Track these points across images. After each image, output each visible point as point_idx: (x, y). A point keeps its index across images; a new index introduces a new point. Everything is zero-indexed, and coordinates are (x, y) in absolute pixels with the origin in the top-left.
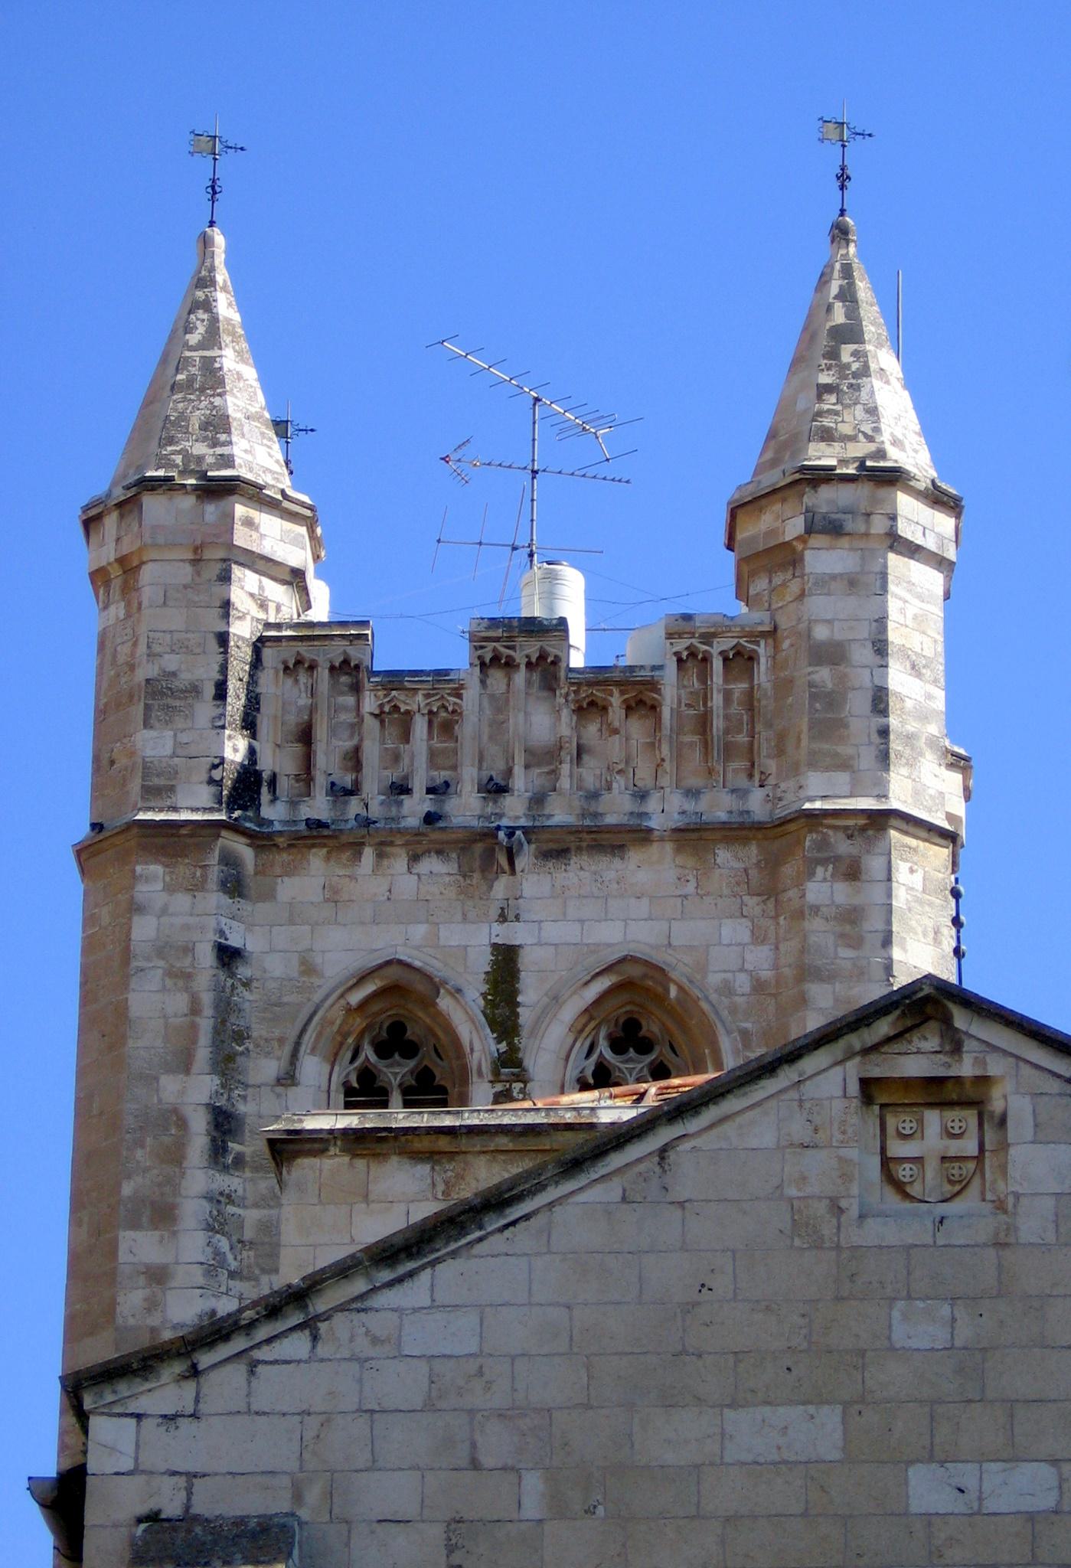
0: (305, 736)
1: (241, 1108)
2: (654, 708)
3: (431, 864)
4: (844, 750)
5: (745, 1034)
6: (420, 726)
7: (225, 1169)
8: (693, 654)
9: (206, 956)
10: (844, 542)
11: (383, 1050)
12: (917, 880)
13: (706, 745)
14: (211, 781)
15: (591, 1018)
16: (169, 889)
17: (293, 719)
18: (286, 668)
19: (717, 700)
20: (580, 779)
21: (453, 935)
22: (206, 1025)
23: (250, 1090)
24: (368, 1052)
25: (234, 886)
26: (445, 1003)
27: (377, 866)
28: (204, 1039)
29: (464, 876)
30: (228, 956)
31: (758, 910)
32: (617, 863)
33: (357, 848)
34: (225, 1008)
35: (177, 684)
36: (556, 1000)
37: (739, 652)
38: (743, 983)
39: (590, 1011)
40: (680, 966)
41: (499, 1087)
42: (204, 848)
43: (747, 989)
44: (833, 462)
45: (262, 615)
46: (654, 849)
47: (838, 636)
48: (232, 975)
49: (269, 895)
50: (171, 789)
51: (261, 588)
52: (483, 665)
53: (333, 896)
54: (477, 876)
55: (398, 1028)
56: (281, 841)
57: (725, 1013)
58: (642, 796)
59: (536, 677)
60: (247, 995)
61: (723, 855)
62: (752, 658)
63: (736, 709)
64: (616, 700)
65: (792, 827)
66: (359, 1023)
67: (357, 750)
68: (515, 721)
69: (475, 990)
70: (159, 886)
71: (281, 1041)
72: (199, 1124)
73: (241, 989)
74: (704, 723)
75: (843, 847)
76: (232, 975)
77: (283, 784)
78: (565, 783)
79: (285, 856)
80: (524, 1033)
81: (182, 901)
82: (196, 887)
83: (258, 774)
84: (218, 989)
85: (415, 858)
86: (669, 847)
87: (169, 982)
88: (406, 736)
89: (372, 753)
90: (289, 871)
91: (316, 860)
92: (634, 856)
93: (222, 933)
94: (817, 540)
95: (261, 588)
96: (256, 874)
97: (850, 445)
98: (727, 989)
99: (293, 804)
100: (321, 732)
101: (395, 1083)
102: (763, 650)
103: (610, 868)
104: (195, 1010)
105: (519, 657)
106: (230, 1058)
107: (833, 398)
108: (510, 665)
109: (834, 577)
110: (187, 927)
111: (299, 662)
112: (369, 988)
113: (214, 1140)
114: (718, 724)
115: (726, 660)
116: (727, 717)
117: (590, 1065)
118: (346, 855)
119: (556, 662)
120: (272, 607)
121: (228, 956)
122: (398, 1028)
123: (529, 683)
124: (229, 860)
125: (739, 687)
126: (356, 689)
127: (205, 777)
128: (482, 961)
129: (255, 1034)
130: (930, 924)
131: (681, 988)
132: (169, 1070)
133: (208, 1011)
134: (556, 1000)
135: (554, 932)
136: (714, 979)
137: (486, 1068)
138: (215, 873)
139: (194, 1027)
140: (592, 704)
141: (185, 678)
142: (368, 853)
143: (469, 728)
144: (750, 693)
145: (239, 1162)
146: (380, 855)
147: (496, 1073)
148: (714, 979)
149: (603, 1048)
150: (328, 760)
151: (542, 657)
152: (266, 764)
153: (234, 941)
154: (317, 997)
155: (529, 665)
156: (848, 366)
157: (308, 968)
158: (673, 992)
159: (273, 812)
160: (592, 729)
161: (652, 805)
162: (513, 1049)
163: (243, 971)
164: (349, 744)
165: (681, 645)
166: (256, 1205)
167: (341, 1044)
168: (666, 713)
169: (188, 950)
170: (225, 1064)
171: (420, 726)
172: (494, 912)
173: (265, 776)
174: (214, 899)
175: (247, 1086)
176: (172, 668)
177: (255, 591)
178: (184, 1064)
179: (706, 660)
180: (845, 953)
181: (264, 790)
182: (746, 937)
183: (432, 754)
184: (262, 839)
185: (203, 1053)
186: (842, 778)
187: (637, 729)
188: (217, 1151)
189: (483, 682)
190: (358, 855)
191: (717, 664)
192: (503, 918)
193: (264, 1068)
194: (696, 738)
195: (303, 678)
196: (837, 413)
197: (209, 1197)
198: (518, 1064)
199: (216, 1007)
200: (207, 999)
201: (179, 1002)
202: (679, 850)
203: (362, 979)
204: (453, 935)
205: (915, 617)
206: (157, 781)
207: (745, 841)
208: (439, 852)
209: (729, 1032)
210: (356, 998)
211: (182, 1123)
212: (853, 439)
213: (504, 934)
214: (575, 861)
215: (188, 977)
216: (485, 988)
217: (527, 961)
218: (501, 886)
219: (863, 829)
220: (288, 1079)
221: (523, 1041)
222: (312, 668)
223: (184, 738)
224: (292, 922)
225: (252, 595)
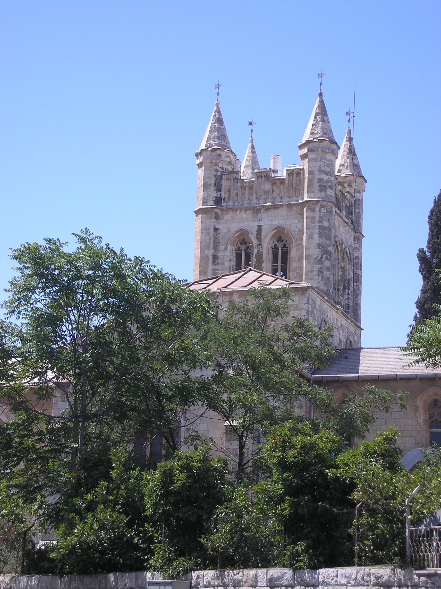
0: (229, 191)
1: (218, 254)
2: (284, 183)
3: (248, 212)
4: (313, 189)
5: (297, 238)
6: (247, 189)
7: (215, 265)
8: (291, 173)
9: (212, 230)
10: (314, 153)
11: (241, 244)
12: (325, 211)
13: (293, 189)
14: (213, 200)
15: (273, 237)
16: (206, 219)
17: (227, 188)
18: (227, 179)
19: (294, 181)
20: (273, 196)
21: (251, 224)
22: (212, 241)
23: (220, 252)
24: (239, 244)
25: (217, 217)
26: (250, 235)
27: (240, 213)
28: (212, 244)
29: (253, 214)
30: (216, 230)
31: (299, 217)
32: (277, 210)
33: (237, 210)
34: (215, 238)
35: (208, 184)
36: (267, 235)
37: (298, 172)
38: (297, 230)
39: (273, 236)
40: (287, 227)
41: (258, 249)
42: (212, 211)
43: (297, 231)
44: (312, 139)
45: (223, 171)
46: (283, 208)
47: (312, 170)
48: (217, 233)
49: (223, 218)
50: (207, 202)
51: (222, 166)
52: (257, 177)
53: (233, 218)
54: (255, 214)
55: (244, 240)
56: (225, 209)
57: (294, 235)
58: (282, 198)
59: (266, 178)
60: (220, 236)
61: (294, 208)
62: (300, 173)
63: (298, 182)
64: (278, 182)
65: (304, 203)
66: (237, 239)
67: (238, 192)
68: (262, 186)
69: (255, 233)
70: (205, 218)
71: (225, 243)
72: (211, 258)
73: (218, 235)
74: (292, 185)
75: (313, 206)
76: (217, 233)
77: (226, 199)
78: (270, 197)
79: (226, 212)
80: (262, 240)
81: (208, 221)
82: (211, 218)
83: (221, 198)
84: (214, 235)
85: (246, 211)
86: (286, 207)
87: (206, 235)
88: (245, 190)
89: (239, 193)
90: (226, 214)
91: (230, 212)
92: (280, 209)
93: (215, 226)
94: (310, 153)
95: (222, 166)
96: (221, 215)
97: (316, 135)
98: (294, 231)
99: (227, 203)
100: (232, 190)
101: (243, 249)
102: (302, 172)
103: (276, 211)
104: (210, 239)
105: (263, 176)
106: (216, 246)
107: (314, 126)
108: (262, 177)
109: (312, 159)
110: (209, 225)
111: (228, 178)
112: (238, 234)
113: (213, 260)
114: (294, 185)
115: (296, 174)
116: (296, 184)
117: (274, 244)
118: (235, 211)
119: (269, 176)
120: (224, 169)
121: (216, 230)
122: (244, 240)
123: (265, 179)
124: (216, 213)
125: (298, 179)
126: (238, 182)
127: (212, 199)
128: (256, 228)
129: (221, 242)
130: (327, 218)
131: (287, 231)
132: (207, 249)
133: (212, 239)
134: (267, 235)
135: (268, 223)
136: (292, 229)
137: (256, 246)
138: (214, 216)
139: (210, 242)
140: (275, 183)
141: (209, 183)
142: (238, 210)
143: (254, 189)
144: (300, 179)
145: (218, 263)
146: (240, 211)
147: (257, 247)
148: (292, 229)
149: (276, 242)
150: (233, 194)
151: (267, 175)
152: (223, 197)
153: (217, 227)
154: (230, 235)
155: (265, 177)
156: (318, 120)
157: (229, 231)
158: (286, 232)
159: (224, 204)
160: (275, 187)
161: (283, 200)
162: (260, 243)
163: (218, 232)
164: (237, 192)
165: (289, 172)
166: (221, 270)
167: (234, 243)
168: (286, 184)
169: (209, 229)
170: (216, 247)
171: (247, 189)
172: (258, 220)
173: (223, 198)
174: (213, 220)
175: (219, 251)
176: (207, 181)
177: (221, 167)
178: (209, 249)
179: (293, 174)
180: (312, 224)
181: (223, 201)
182: (297, 222)
183: (249, 192)
184: (222, 210)
185: (212, 246)
186: (313, 194)
187: (282, 187)
188: (214, 263)
189: (257, 180)
190: (237, 211)
191: (295, 175)
192: (259, 221)
193: (222, 248)
194: (291, 188)
195: (229, 181)
196: (315, 129)
197: (212, 270)
198: (261, 245)
199: (214, 238)
200: (212, 237)
201: (208, 238)
202: (287, 208)
203: (237, 232)
204: (251, 224)
205: (327, 165)
206: (205, 201)
207: (298, 206)
208: (249, 210)
209: (294, 238)
210: (236, 235)
211: (208, 258)
212: (317, 134)
213: (260, 223)
214: (271, 211)
215: (209, 233)
216: (256, 233)
217: (263, 228)
218: (259, 216)
219: (316, 203)
220: (226, 249)
221: (262, 241)
222: (231, 179)
223: (209, 193)
224: (226, 223)
225: (220, 167)
